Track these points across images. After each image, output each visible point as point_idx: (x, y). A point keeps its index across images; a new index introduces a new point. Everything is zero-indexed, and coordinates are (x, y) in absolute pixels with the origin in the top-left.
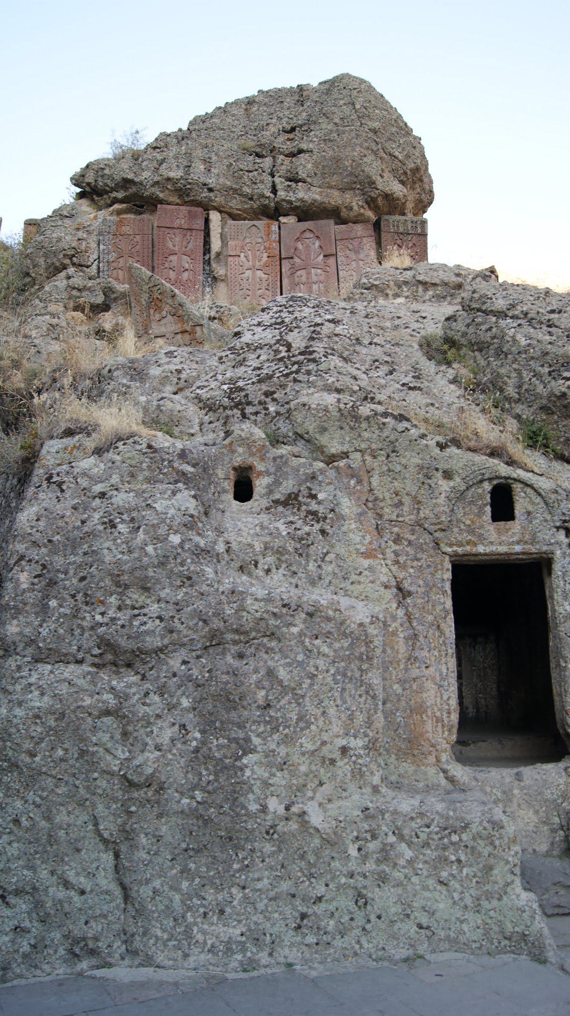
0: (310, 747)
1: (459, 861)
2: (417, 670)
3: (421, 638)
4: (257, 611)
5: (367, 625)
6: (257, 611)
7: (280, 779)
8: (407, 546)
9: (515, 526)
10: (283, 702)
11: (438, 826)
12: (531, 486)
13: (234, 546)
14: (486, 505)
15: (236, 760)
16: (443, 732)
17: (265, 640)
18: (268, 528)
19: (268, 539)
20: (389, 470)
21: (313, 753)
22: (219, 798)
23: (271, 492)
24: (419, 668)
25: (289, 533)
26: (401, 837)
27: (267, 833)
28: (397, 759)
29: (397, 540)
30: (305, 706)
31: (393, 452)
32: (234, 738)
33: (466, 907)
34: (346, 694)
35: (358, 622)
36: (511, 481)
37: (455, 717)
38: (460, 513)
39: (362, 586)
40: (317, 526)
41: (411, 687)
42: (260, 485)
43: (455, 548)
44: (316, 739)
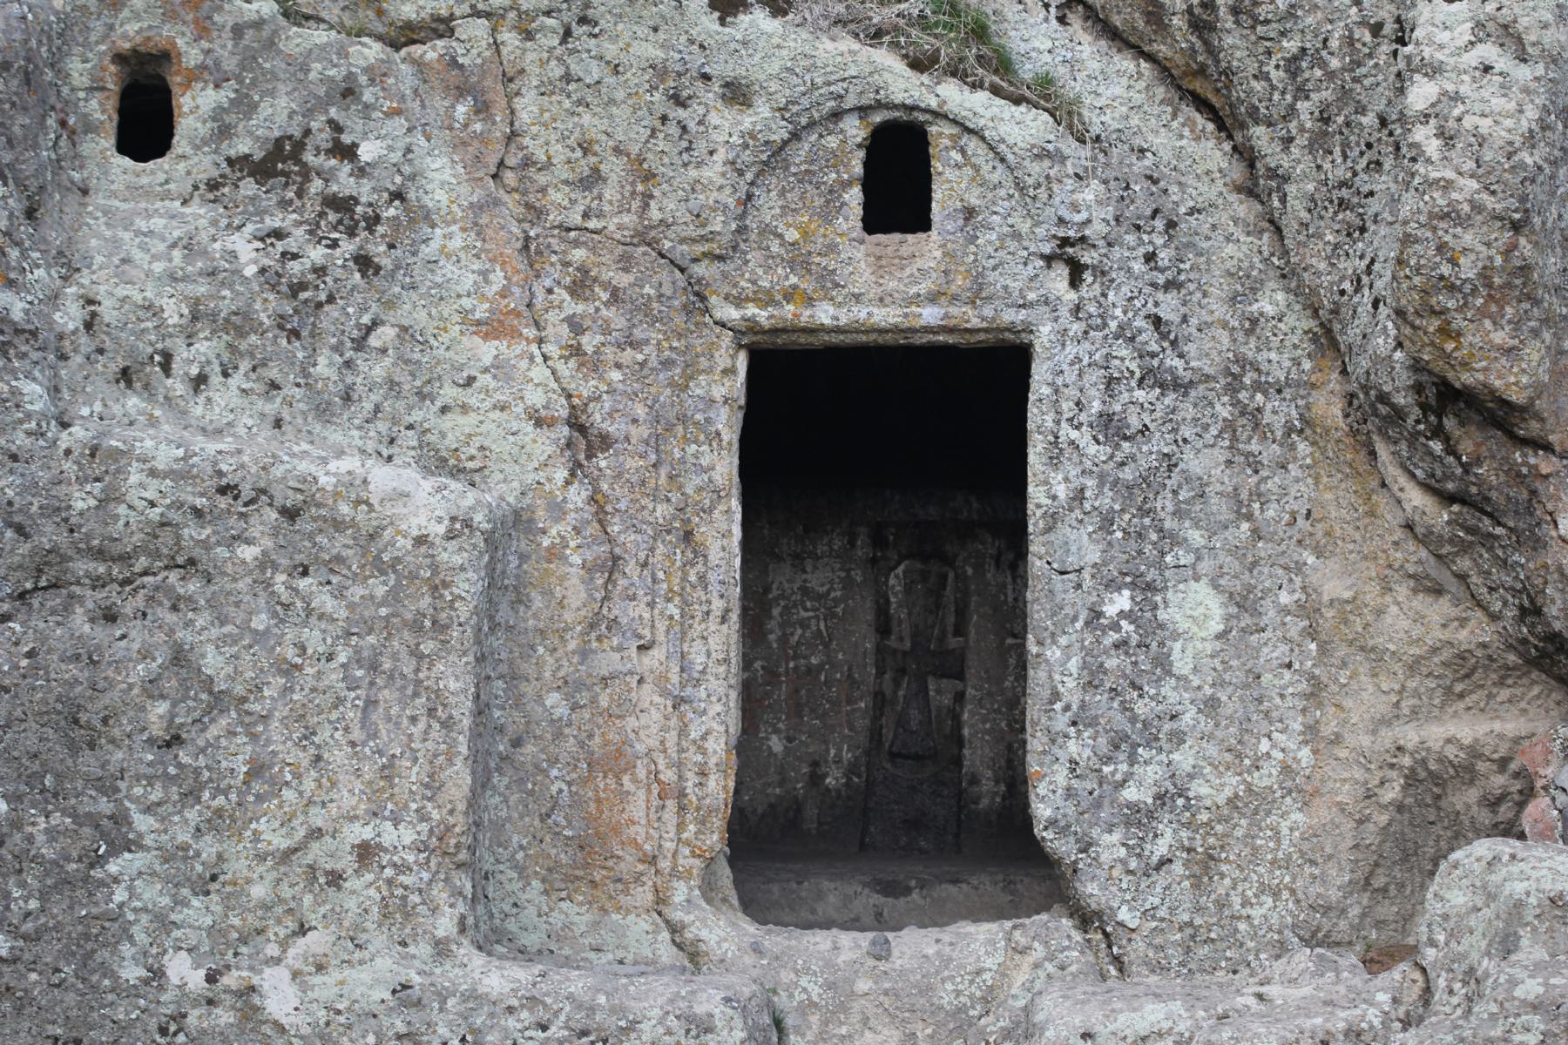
0: (280, 842)
2: (617, 656)
3: (631, 568)
4: (152, 504)
5: (437, 541)
6: (152, 504)
7: (198, 913)
8: (607, 304)
9: (926, 250)
10: (213, 731)
11: (567, 1027)
13: (108, 311)
14: (849, 184)
15: (92, 866)
16: (681, 827)
17: (173, 577)
18: (205, 253)
19: (202, 289)
20: (567, 78)
21: (287, 855)
22: (49, 952)
23: (224, 132)
24: (620, 649)
25: (263, 271)
27: (163, 1031)
28: (546, 892)
29: (579, 288)
30: (268, 742)
31: (583, 20)
32: (89, 815)
34: (376, 716)
35: (415, 533)
36: (922, 117)
37: (718, 789)
38: (769, 205)
39: (472, 418)
40: (348, 247)
41: (594, 700)
42: (195, 107)
43: (751, 310)
44: (295, 823)
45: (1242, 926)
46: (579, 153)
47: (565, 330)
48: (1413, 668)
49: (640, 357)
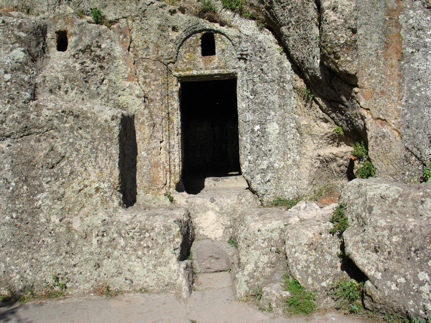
1: (148, 247)
4: (47, 116)
7: (58, 206)
12: (223, 34)
17: (51, 131)
23: (77, 45)
26: (120, 235)
31: (144, 17)
33: (149, 269)
34: (98, 159)
40: (98, 64)
41: (152, 153)
42: (71, 40)
43: (180, 73)
44: (81, 184)
45: (286, 193)
46: (144, 43)
47: (143, 79)
48: (321, 138)
49: (158, 83)
